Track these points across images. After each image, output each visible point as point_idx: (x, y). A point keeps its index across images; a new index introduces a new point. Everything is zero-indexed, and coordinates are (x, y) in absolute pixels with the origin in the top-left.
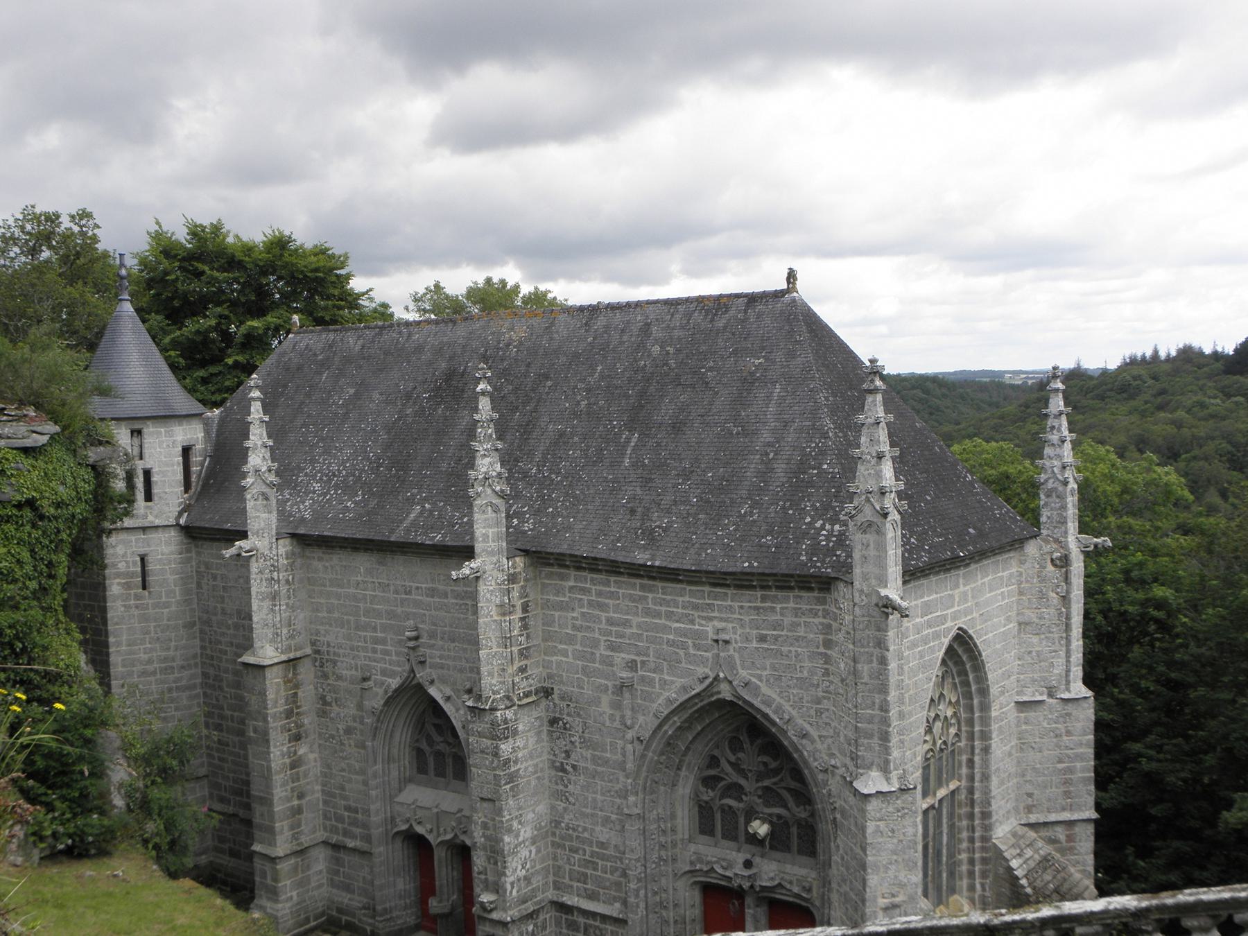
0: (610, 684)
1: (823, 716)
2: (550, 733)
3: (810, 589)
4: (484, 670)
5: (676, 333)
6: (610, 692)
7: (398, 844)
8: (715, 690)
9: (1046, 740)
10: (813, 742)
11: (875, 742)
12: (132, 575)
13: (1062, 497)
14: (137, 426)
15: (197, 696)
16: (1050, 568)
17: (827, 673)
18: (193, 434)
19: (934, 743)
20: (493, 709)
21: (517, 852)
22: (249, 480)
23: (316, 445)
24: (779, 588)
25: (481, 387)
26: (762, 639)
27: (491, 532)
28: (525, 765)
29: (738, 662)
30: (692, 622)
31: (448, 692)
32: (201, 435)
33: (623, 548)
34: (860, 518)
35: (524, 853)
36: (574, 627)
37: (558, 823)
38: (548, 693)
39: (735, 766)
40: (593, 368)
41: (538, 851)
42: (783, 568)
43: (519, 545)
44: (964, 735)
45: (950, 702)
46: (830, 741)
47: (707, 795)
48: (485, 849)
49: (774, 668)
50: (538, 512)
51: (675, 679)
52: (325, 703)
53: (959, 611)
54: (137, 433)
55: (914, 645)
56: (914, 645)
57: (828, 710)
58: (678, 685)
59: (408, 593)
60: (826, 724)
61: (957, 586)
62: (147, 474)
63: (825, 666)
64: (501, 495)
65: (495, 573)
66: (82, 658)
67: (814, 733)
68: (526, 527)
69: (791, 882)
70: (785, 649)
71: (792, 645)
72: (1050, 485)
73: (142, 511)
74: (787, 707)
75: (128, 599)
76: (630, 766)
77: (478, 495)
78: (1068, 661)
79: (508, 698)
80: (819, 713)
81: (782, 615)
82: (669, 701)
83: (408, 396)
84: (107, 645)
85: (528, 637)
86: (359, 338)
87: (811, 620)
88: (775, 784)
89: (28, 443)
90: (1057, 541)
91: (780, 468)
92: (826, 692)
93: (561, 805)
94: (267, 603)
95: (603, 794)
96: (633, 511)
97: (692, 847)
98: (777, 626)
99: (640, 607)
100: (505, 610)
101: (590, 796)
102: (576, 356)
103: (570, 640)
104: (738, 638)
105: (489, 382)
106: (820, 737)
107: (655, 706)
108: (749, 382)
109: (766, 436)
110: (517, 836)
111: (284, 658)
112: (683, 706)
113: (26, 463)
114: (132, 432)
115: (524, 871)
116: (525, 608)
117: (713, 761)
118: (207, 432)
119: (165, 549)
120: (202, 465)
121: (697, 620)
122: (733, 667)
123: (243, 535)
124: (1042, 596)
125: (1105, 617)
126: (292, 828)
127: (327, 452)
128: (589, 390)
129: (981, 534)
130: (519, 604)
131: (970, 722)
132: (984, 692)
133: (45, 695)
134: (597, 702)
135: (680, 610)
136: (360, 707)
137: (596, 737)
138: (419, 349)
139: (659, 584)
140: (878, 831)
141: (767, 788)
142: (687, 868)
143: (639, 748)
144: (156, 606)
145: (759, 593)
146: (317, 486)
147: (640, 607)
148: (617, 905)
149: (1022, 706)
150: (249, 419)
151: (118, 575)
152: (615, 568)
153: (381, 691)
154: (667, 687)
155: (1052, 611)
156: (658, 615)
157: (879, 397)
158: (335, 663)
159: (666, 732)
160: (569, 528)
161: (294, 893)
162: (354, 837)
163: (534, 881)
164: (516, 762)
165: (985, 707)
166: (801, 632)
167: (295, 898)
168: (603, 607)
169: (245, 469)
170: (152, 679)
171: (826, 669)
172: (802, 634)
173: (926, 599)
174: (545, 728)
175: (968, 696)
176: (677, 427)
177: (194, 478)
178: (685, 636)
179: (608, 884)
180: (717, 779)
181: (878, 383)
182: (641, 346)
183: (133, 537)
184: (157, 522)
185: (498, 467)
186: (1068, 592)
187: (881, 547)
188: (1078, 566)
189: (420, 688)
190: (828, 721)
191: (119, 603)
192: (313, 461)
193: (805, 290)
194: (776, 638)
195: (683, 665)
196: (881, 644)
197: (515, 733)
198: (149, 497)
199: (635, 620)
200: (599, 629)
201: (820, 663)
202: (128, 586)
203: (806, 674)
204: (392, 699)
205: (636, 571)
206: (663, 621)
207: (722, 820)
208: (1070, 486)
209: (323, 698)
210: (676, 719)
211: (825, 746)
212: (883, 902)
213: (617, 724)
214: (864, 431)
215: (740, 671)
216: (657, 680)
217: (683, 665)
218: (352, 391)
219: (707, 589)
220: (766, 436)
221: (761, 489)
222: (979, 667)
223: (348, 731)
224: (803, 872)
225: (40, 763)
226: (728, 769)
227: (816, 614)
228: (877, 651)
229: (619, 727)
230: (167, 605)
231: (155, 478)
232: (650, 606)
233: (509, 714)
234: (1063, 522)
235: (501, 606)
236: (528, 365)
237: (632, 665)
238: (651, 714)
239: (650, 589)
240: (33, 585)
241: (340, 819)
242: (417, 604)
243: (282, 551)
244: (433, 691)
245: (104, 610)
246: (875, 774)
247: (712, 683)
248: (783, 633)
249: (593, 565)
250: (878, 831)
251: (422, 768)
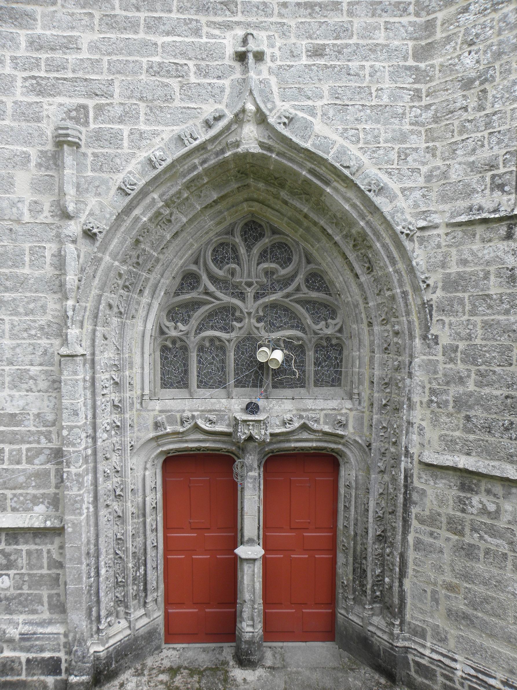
0: (33, 152)
1: (409, 159)
6: (33, 164)
8: (232, 139)
10: (392, 198)
29: (275, 89)
30: (197, 32)
46: (417, 194)
51: (160, 128)
57: (416, 150)
58: (166, 136)
60: (413, 170)
63: (416, 86)
67: (394, 186)
69: (317, 421)
70: (354, 65)
71: (365, 58)
80: (403, 155)
81: (350, 13)
87: (397, 19)
88: (288, 296)
92: (416, 123)
95: (13, 336)
97: (157, 406)
99: (97, 15)
104: (278, 53)
106: (403, 190)
107: (119, 178)
121: (205, 29)
135: (174, 15)
141: (274, 306)
142: (152, 435)
147: (97, 15)
148: (40, 509)
154: (144, 142)
156: (134, 26)
159: (137, 219)
166: (380, 38)
171: (418, 91)
172: (382, 41)
178: (183, 54)
179: (22, 479)
190: (416, 165)
195: (177, 103)
200: (14, 59)
201: (407, 82)
203: (385, 100)
206: (141, 35)
207: (199, 362)
210: (156, 196)
211: (411, 202)
213: (45, 216)
215: (278, 103)
216: (126, 134)
217: (177, 103)
224: (333, 404)
227: (405, 10)
229: (50, 220)
232: (118, 11)
238: (113, 190)
247: (228, 128)
248: (351, 42)
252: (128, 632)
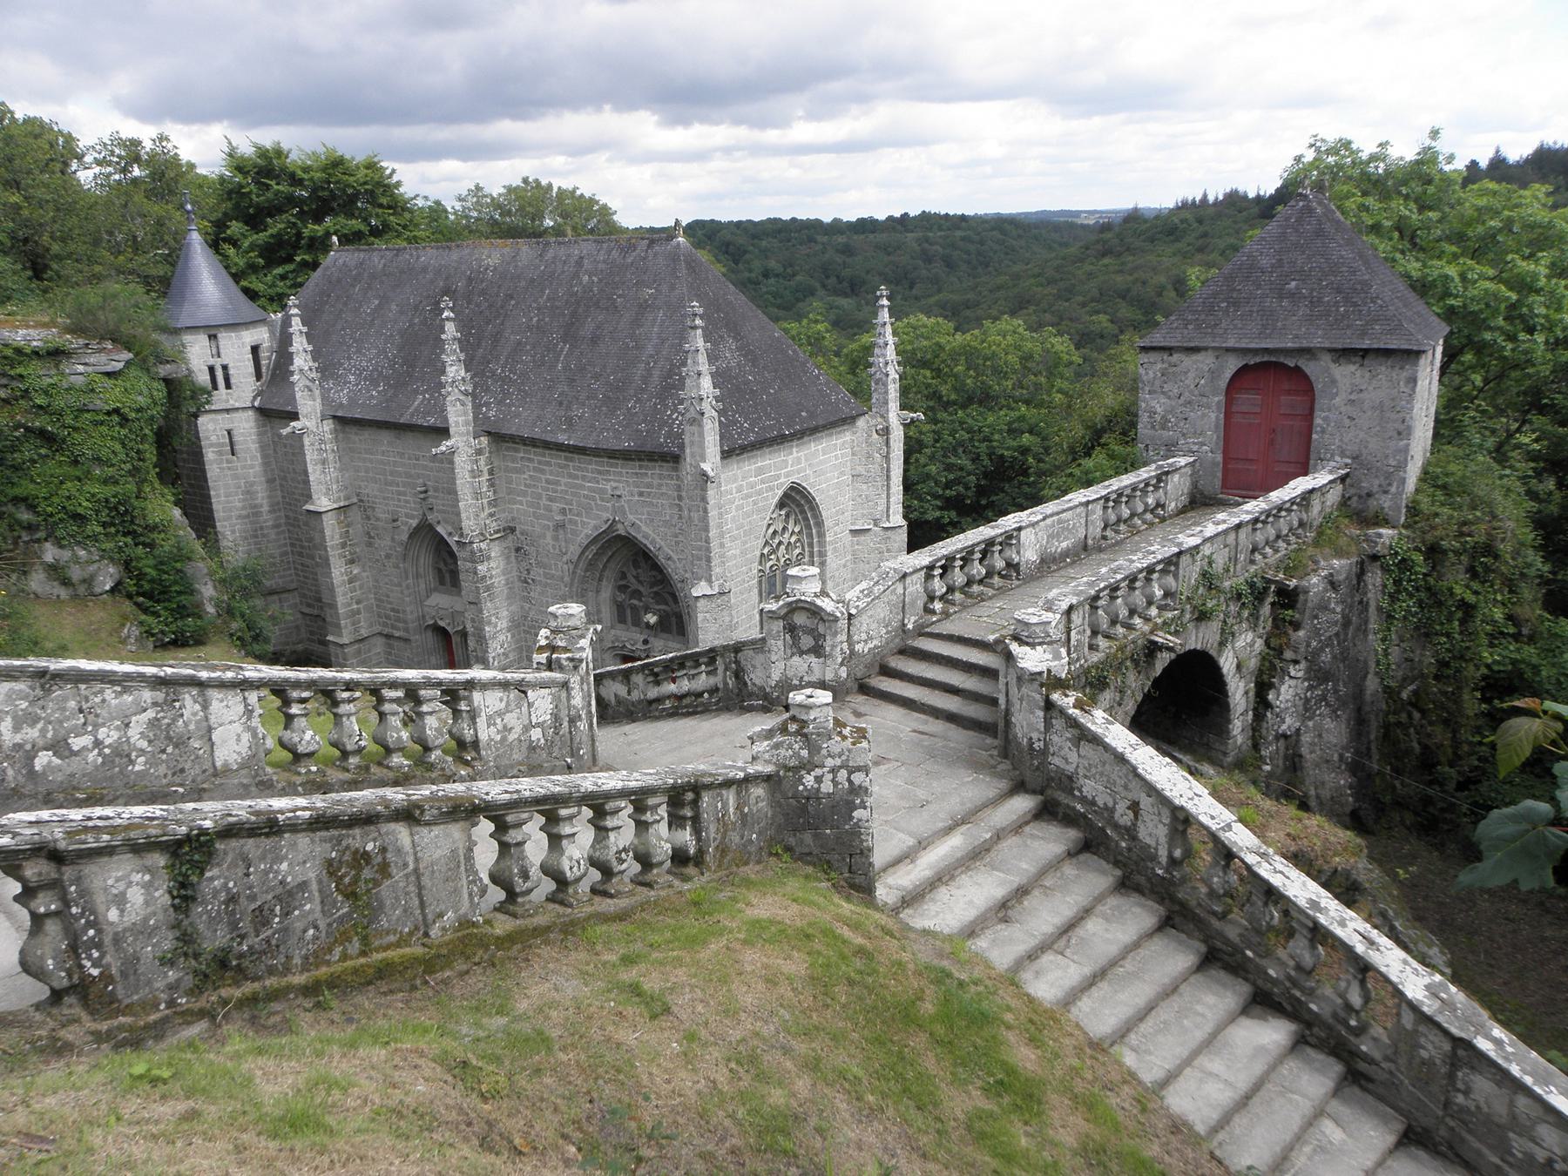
0: (551, 524)
2: (516, 557)
3: (668, 462)
4: (463, 516)
5: (601, 266)
7: (429, 634)
9: (872, 555)
10: (674, 562)
11: (704, 563)
12: (222, 445)
13: (885, 385)
14: (212, 332)
15: (283, 532)
16: (876, 436)
17: (680, 517)
18: (261, 335)
19: (778, 560)
20: (472, 543)
22: (296, 377)
23: (350, 345)
24: (649, 460)
25: (446, 314)
26: (641, 494)
27: (461, 419)
30: (598, 482)
31: (450, 529)
32: (266, 336)
33: (551, 431)
34: (688, 416)
35: (502, 637)
36: (526, 485)
37: (526, 617)
38: (513, 530)
39: (636, 578)
40: (543, 291)
42: (648, 448)
43: (484, 428)
44: (807, 554)
45: (793, 532)
47: (621, 597)
48: (474, 635)
49: (649, 514)
50: (500, 403)
52: (370, 537)
55: (748, 496)
56: (748, 496)
59: (417, 459)
62: (225, 368)
64: (466, 393)
65: (466, 448)
66: (177, 513)
67: (675, 557)
68: (491, 413)
72: (878, 376)
73: (224, 397)
74: (658, 540)
75: (221, 462)
76: (567, 579)
77: (449, 393)
78: (888, 501)
79: (482, 534)
80: (677, 543)
82: (587, 536)
83: (416, 308)
84: (209, 497)
85: (495, 492)
86: (382, 257)
89: (109, 369)
90: (882, 416)
91: (656, 373)
93: (527, 606)
94: (319, 467)
96: (561, 404)
97: (613, 632)
98: (649, 486)
100: (475, 474)
101: (545, 600)
102: (532, 281)
103: (524, 494)
105: (452, 309)
108: (644, 307)
109: (650, 350)
110: (496, 626)
111: (336, 506)
112: (594, 540)
113: (110, 383)
114: (210, 337)
116: (491, 472)
117: (623, 576)
118: (272, 333)
119: (247, 425)
120: (270, 358)
122: (625, 513)
123: (294, 416)
124: (869, 456)
125: (991, 460)
126: (353, 624)
127: (359, 351)
128: (539, 309)
129: (812, 415)
130: (485, 469)
131: (811, 545)
132: (820, 524)
133: (148, 541)
134: (544, 536)
136: (393, 539)
137: (545, 560)
138: (424, 270)
139: (576, 456)
140: (705, 619)
141: (656, 593)
143: (572, 567)
144: (244, 467)
145: (637, 464)
146: (352, 378)
149: (855, 532)
150: (291, 330)
151: (212, 445)
152: (547, 445)
153: (406, 528)
155: (877, 466)
156: (576, 477)
157: (699, 332)
158: (374, 508)
160: (518, 415)
162: (398, 629)
164: (491, 578)
165: (821, 535)
168: (542, 472)
169: (292, 368)
174: (513, 554)
175: (809, 527)
176: (595, 340)
177: (264, 369)
180: (626, 587)
181: (698, 322)
182: (576, 275)
183: (219, 417)
184: (237, 405)
185: (463, 373)
186: (888, 453)
187: (701, 435)
188: (898, 435)
189: (431, 528)
191: (215, 466)
192: (349, 358)
194: (649, 494)
196: (704, 500)
197: (489, 558)
198: (228, 386)
199: (563, 480)
201: (675, 511)
202: (220, 453)
204: (415, 533)
205: (560, 447)
208: (890, 378)
209: (368, 533)
213: (557, 551)
214: (690, 355)
218: (377, 302)
219: (606, 460)
220: (650, 350)
221: (642, 389)
222: (814, 507)
223: (388, 556)
225: (147, 586)
226: (633, 580)
228: (702, 504)
230: (252, 467)
231: (231, 372)
233: (483, 545)
234: (886, 403)
235: (473, 471)
236: (499, 287)
237: (563, 512)
239: (572, 460)
240: (128, 466)
241: (388, 617)
242: (425, 467)
243: (326, 428)
244: (439, 529)
245: (204, 471)
246: (703, 583)
249: (533, 443)
250: (705, 619)
251: (442, 582)
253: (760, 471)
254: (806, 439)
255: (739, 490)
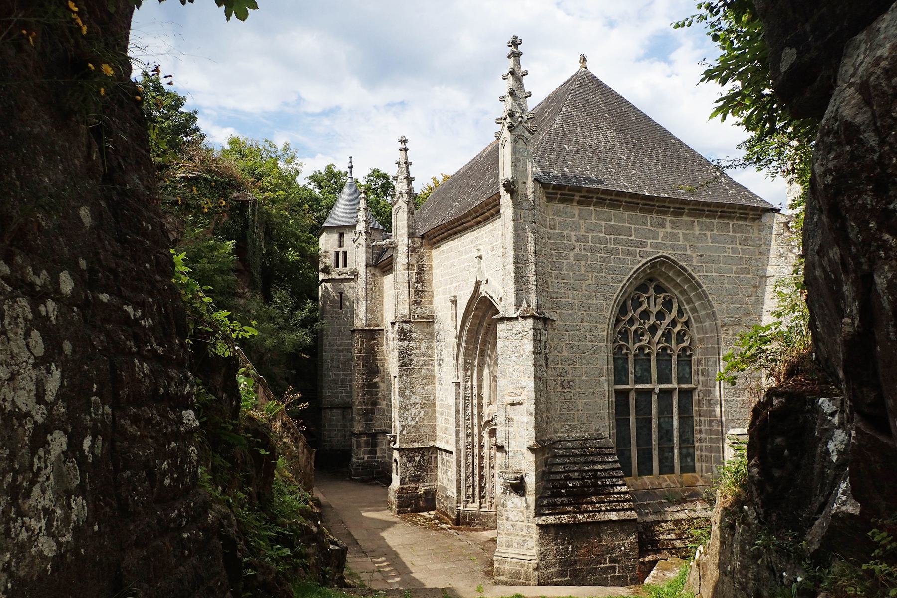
21: (409, 409)
28: (416, 359)
41: (426, 414)
53: (664, 244)
54: (341, 235)
55: (592, 250)
61: (663, 226)
62: (345, 253)
115: (413, 422)
161: (366, 457)
163: (421, 430)
167: (366, 459)
170: (341, 354)
173: (613, 223)
193: (597, 70)
198: (345, 265)
212: (510, 400)
233: (406, 326)
252: (476, 509)
253: (612, 230)
254: (685, 218)
255: (581, 239)
